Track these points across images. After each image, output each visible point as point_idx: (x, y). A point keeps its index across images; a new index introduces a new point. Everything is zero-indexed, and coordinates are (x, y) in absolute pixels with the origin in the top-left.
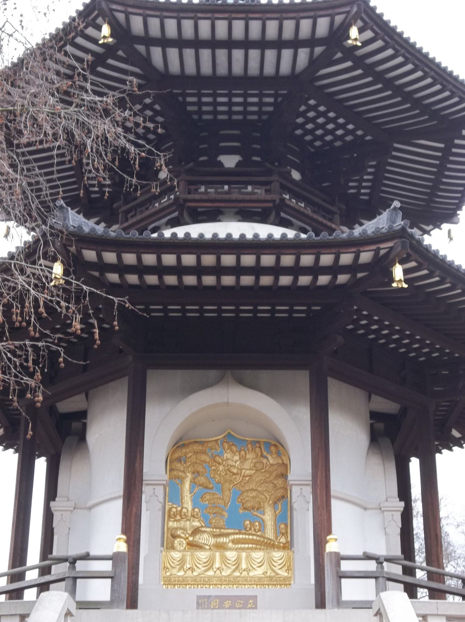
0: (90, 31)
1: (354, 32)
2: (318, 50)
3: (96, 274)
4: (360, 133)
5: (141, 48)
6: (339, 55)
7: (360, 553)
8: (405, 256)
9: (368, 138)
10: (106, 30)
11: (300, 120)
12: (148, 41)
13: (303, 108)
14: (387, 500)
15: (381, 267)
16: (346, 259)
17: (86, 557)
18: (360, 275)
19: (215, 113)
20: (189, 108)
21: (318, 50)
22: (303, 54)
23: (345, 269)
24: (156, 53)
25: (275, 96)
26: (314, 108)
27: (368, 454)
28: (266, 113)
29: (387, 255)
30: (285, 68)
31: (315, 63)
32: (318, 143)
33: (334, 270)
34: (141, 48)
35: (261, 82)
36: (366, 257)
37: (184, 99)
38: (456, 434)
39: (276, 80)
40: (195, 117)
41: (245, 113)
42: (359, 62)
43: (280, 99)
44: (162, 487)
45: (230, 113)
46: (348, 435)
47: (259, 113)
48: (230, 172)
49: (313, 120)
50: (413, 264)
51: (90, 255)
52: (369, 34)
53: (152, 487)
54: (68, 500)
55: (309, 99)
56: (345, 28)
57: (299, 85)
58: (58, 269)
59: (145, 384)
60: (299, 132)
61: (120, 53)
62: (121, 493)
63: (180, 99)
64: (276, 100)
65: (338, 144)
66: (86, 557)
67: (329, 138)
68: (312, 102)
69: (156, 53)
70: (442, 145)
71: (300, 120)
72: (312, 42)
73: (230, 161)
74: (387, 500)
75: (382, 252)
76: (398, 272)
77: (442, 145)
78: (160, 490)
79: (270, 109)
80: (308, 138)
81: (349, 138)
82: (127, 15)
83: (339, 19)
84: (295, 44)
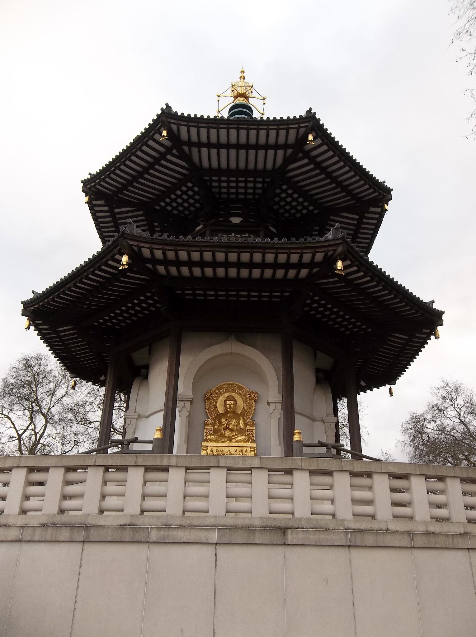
1: (311, 137)
2: (289, 151)
3: (150, 266)
4: (311, 208)
5: (186, 148)
6: (301, 155)
8: (343, 256)
9: (316, 211)
10: (165, 133)
11: (277, 199)
12: (190, 144)
13: (278, 191)
16: (307, 258)
17: (135, 440)
18: (315, 270)
19: (228, 193)
20: (214, 190)
21: (289, 151)
22: (280, 153)
23: (305, 266)
24: (195, 150)
25: (263, 182)
26: (285, 191)
28: (258, 194)
29: (332, 255)
30: (269, 166)
31: (287, 161)
32: (287, 215)
33: (299, 266)
34: (186, 148)
35: (255, 173)
36: (319, 257)
37: (211, 184)
38: (363, 383)
39: (264, 172)
40: (217, 196)
41: (246, 194)
42: (312, 160)
43: (266, 185)
44: (189, 403)
45: (237, 193)
46: (303, 376)
47: (254, 194)
48: (236, 225)
50: (348, 262)
51: (146, 252)
52: (319, 141)
54: (135, 412)
55: (282, 185)
57: (278, 175)
58: (125, 259)
60: (276, 207)
61: (174, 151)
63: (208, 183)
64: (263, 185)
65: (298, 215)
66: (135, 440)
67: (293, 211)
68: (284, 187)
69: (195, 150)
70: (357, 217)
71: (277, 199)
72: (285, 146)
73: (236, 220)
75: (330, 253)
76: (340, 265)
77: (357, 217)
78: (188, 404)
79: (259, 191)
80: (281, 211)
81: (305, 212)
82: (178, 125)
83: (302, 131)
84: (276, 147)
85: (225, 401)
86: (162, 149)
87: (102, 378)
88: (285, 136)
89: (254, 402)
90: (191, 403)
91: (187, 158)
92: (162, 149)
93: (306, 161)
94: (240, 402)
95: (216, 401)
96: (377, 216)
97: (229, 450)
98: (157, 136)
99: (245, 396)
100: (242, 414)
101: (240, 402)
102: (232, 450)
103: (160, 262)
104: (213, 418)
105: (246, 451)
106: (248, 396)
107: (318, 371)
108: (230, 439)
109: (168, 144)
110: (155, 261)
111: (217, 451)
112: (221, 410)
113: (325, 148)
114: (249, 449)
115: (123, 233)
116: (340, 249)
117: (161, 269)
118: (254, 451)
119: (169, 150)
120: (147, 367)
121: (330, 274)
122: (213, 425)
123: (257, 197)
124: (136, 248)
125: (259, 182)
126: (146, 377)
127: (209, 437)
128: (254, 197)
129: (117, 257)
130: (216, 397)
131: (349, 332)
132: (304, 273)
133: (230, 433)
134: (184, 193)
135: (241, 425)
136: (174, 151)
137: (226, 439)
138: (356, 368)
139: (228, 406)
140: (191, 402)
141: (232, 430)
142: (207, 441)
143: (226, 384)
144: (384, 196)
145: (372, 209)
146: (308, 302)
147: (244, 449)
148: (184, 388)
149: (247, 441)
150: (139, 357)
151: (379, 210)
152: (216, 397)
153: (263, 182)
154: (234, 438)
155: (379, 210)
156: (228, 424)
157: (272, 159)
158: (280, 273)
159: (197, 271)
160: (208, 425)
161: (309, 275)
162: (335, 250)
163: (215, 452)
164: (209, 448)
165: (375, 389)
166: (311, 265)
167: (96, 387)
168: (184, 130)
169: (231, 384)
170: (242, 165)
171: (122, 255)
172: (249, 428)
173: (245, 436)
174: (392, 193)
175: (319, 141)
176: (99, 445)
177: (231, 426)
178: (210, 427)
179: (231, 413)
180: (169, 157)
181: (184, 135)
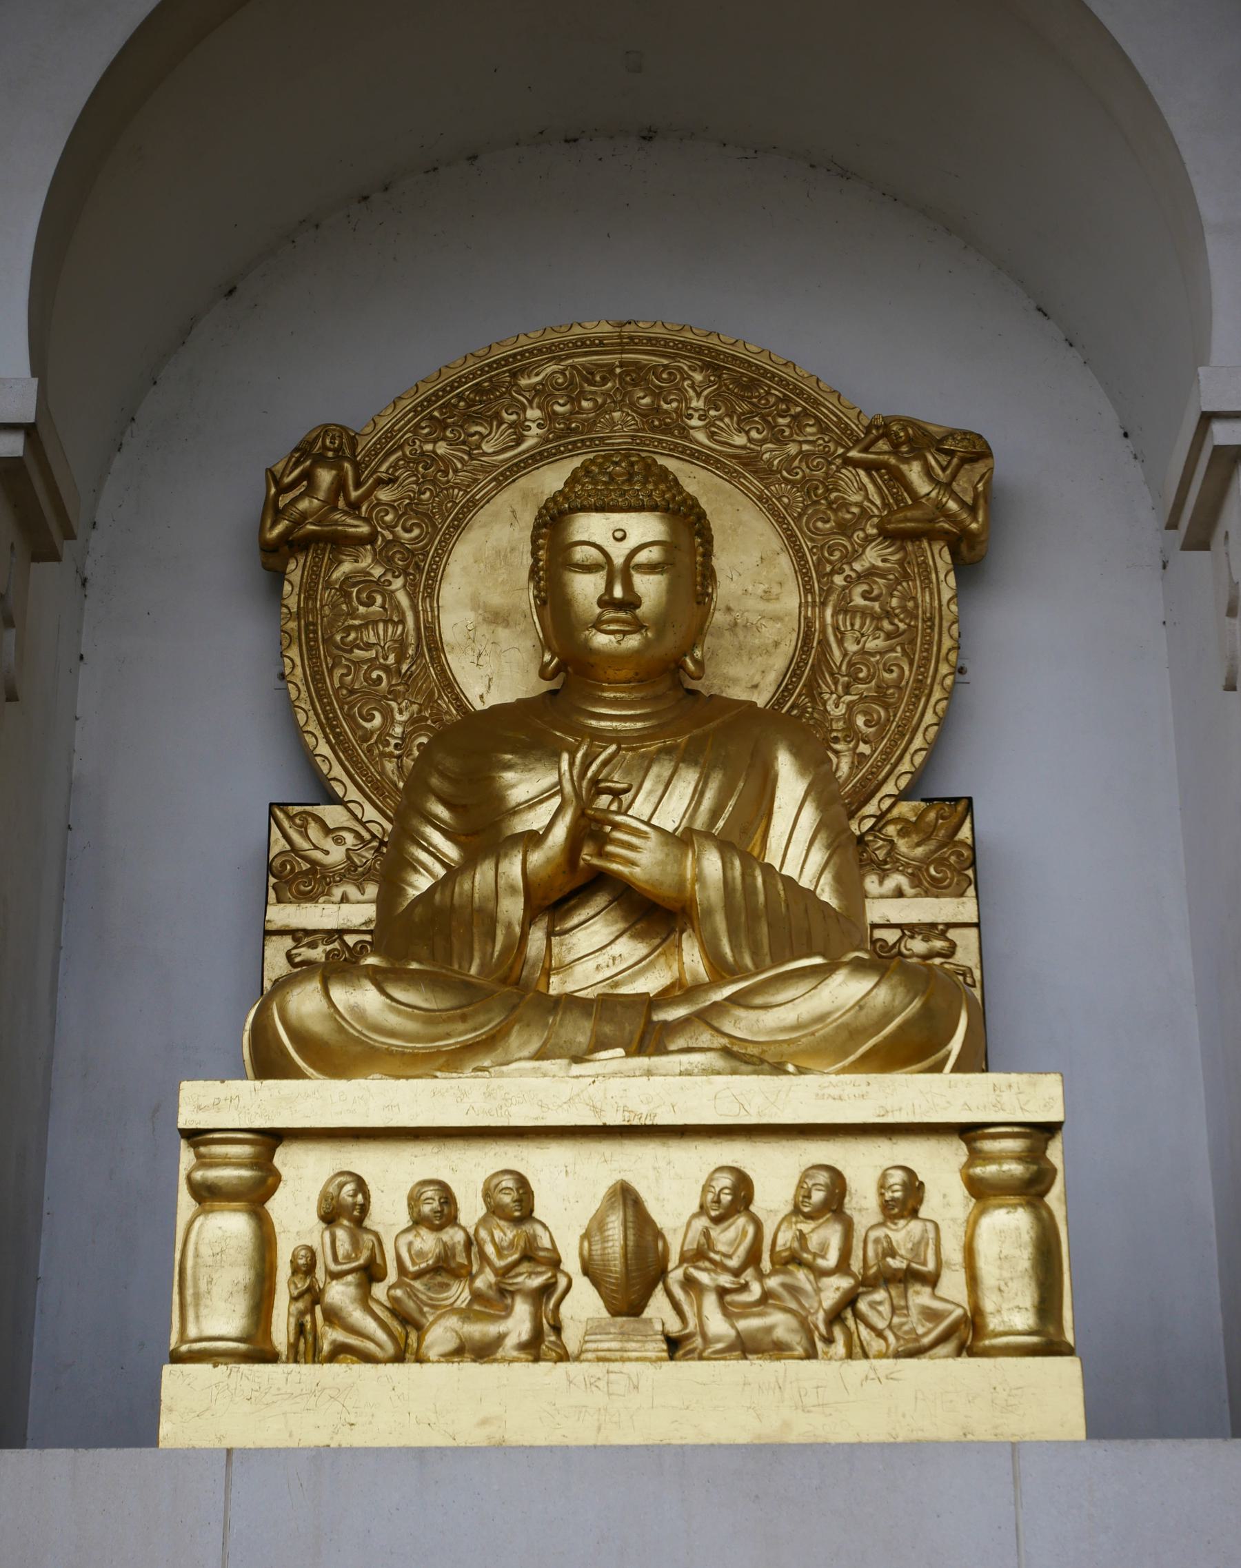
85: (552, 523)
89: (941, 558)
94: (754, 570)
95: (423, 571)
97: (626, 1197)
99: (819, 492)
100: (794, 718)
101: (754, 570)
102: (674, 1186)
104: (376, 789)
105: (906, 1200)
106: (860, 490)
108: (638, 1027)
111: (437, 1209)
112: (494, 671)
114: (941, 1167)
118: (1032, 1189)
122: (389, 866)
127: (306, 1002)
130: (410, 510)
133: (629, 950)
135: (794, 842)
137: (580, 1032)
139: (586, 589)
141: (655, 915)
142: (269, 1064)
143: (553, 352)
147: (865, 1166)
149: (913, 1048)
152: (410, 510)
154: (705, 1017)
156: (590, 829)
160: (307, 881)
163: (389, 1214)
164: (304, 1176)
169: (627, 343)
172: (890, 906)
173: (859, 967)
177: (643, 862)
178: (353, 911)
179: (644, 684)
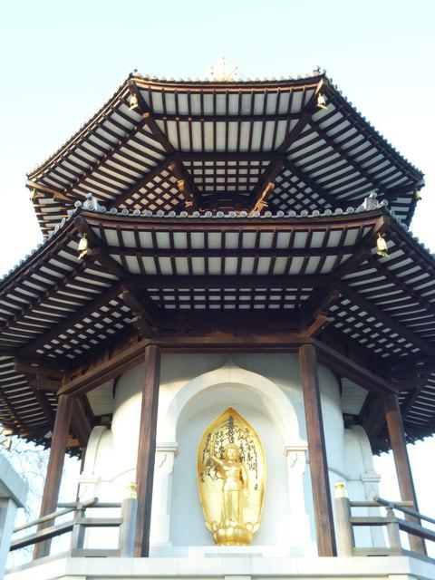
0: (123, 108)
2: (294, 122)
3: (117, 257)
5: (160, 123)
7: (371, 500)
12: (167, 116)
14: (366, 472)
15: (367, 241)
16: (335, 238)
18: (346, 257)
20: (198, 180)
21: (294, 122)
22: (282, 124)
23: (332, 251)
24: (172, 125)
25: (260, 167)
26: (287, 179)
27: (345, 432)
28: (253, 184)
30: (268, 145)
31: (292, 136)
33: (324, 251)
35: (250, 155)
36: (352, 237)
37: (192, 172)
39: (261, 154)
40: (200, 188)
42: (323, 133)
43: (263, 171)
44: (172, 454)
47: (248, 184)
49: (286, 191)
50: (392, 244)
51: (111, 236)
53: (165, 453)
55: (285, 170)
56: (315, 98)
57: (278, 158)
58: (83, 244)
59: (160, 362)
61: (146, 127)
62: (135, 466)
63: (189, 171)
68: (287, 173)
72: (288, 116)
74: (366, 472)
76: (382, 244)
78: (171, 456)
79: (254, 180)
83: (310, 93)
84: (277, 117)
86: (128, 124)
87: (48, 435)
88: (287, 102)
90: (176, 456)
91: (162, 136)
92: (128, 124)
93: (315, 135)
96: (406, 209)
98: (123, 108)
103: (131, 251)
107: (345, 415)
109: (136, 116)
110: (123, 249)
113: (339, 116)
115: (80, 209)
116: (381, 222)
117: (132, 262)
119: (139, 125)
120: (110, 416)
121: (366, 262)
123: (251, 188)
124: (97, 231)
125: (255, 167)
126: (109, 427)
128: (248, 188)
129: (72, 244)
131: (387, 355)
132: (330, 261)
134: (158, 185)
136: (146, 127)
138: (400, 401)
140: (176, 454)
144: (416, 182)
145: (400, 200)
146: (334, 308)
148: (166, 431)
150: (96, 399)
151: (408, 201)
153: (260, 167)
155: (408, 201)
157: (267, 136)
158: (297, 262)
159: (182, 264)
161: (338, 268)
162: (374, 225)
165: (418, 442)
166: (340, 249)
167: (41, 447)
168: (157, 98)
170: (232, 146)
171: (78, 240)
174: (424, 177)
175: (331, 107)
176: (43, 514)
180: (139, 135)
181: (158, 106)
